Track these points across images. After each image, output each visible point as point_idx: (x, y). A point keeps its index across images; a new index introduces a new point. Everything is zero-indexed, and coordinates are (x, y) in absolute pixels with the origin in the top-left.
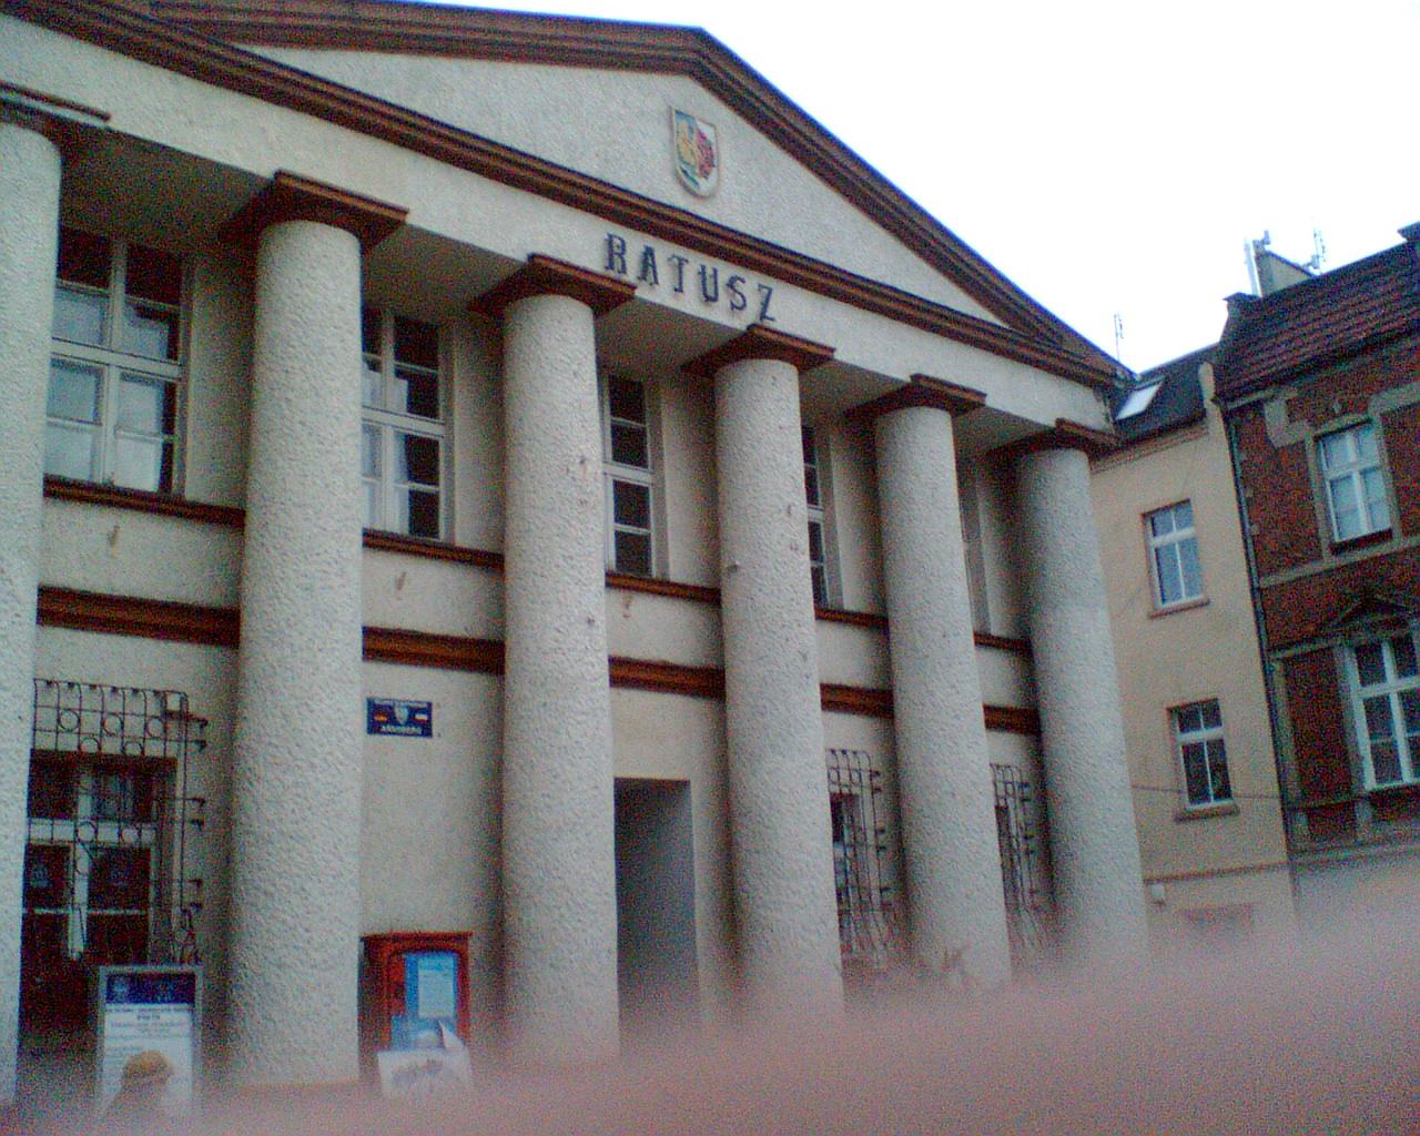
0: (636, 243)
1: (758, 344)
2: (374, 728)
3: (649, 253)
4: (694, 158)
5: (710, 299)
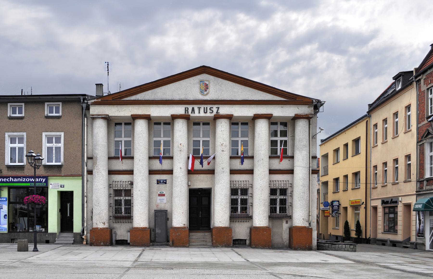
0: (190, 107)
1: (218, 117)
2: (158, 183)
3: (193, 109)
4: (203, 88)
5: (205, 113)
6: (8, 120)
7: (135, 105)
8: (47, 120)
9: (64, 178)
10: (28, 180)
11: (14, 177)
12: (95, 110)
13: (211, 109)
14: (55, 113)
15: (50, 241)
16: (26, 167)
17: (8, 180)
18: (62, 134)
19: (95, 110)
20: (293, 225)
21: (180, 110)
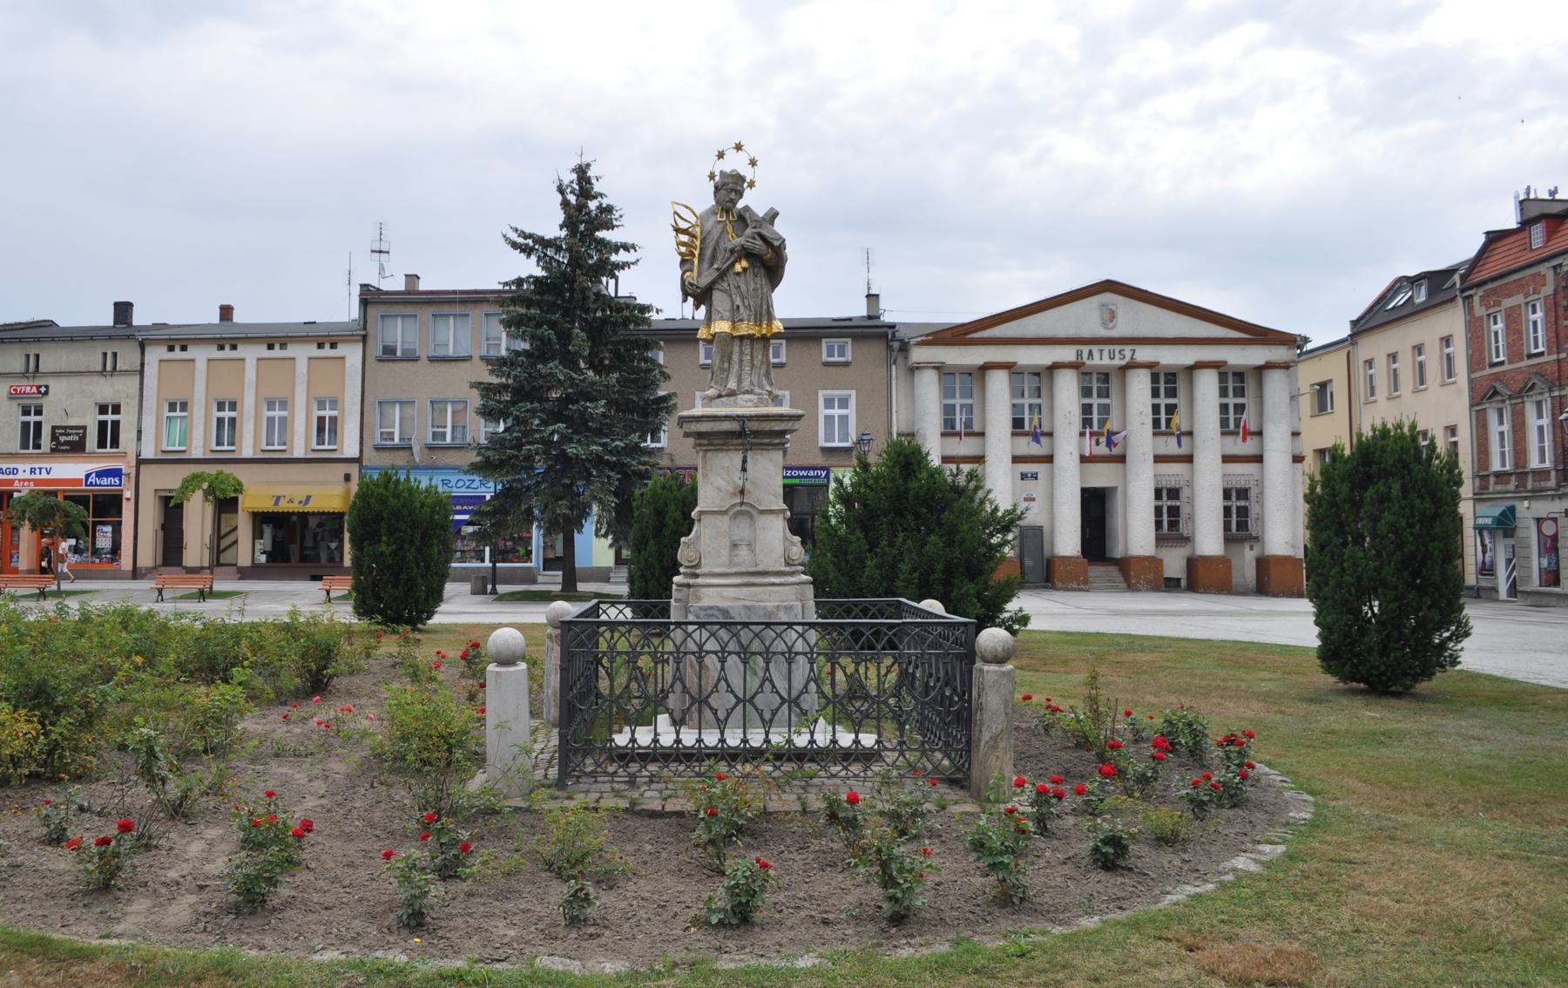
0: (1085, 349)
1: (1133, 365)
2: (1022, 479)
3: (1090, 352)
4: (1107, 316)
12: (919, 355)
19: (919, 355)
20: (1267, 554)
21: (1067, 354)
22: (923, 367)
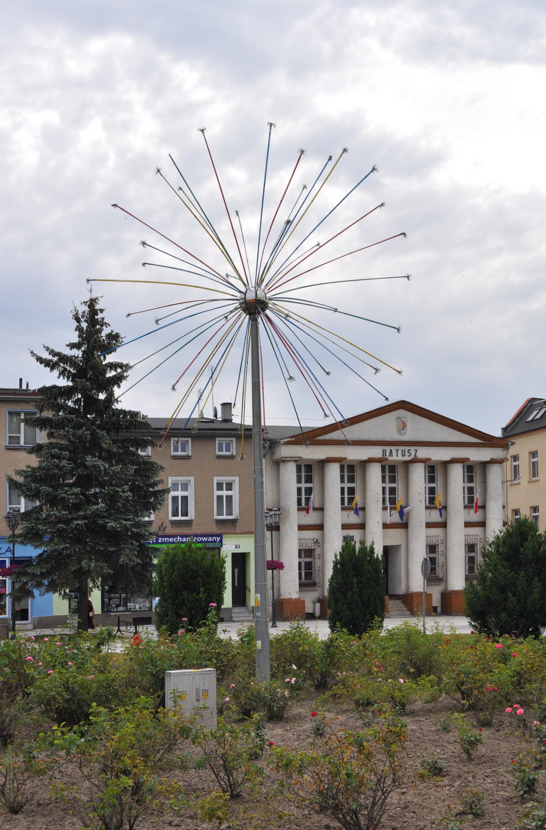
0: (388, 449)
1: (416, 461)
3: (391, 451)
6: (171, 460)
7: (331, 446)
8: (219, 460)
9: (240, 535)
10: (199, 539)
11: (182, 536)
12: (285, 451)
13: (410, 451)
14: (181, 451)
15: (225, 619)
16: (194, 521)
17: (176, 540)
18: (237, 479)
21: (376, 452)
22: (288, 461)
